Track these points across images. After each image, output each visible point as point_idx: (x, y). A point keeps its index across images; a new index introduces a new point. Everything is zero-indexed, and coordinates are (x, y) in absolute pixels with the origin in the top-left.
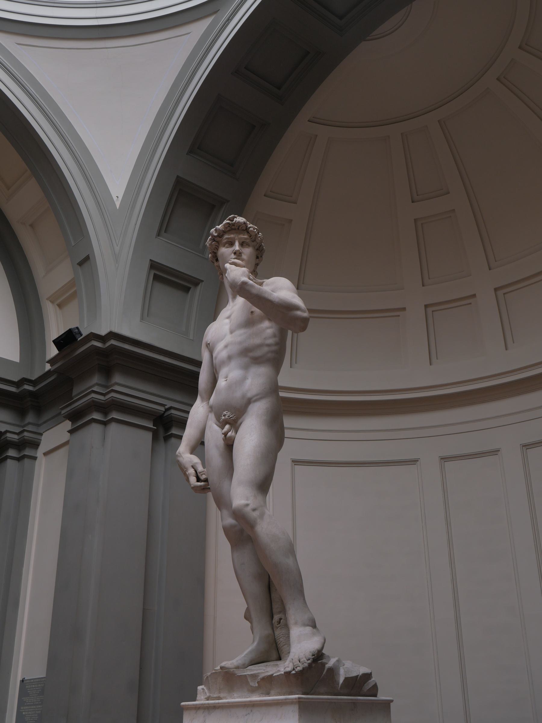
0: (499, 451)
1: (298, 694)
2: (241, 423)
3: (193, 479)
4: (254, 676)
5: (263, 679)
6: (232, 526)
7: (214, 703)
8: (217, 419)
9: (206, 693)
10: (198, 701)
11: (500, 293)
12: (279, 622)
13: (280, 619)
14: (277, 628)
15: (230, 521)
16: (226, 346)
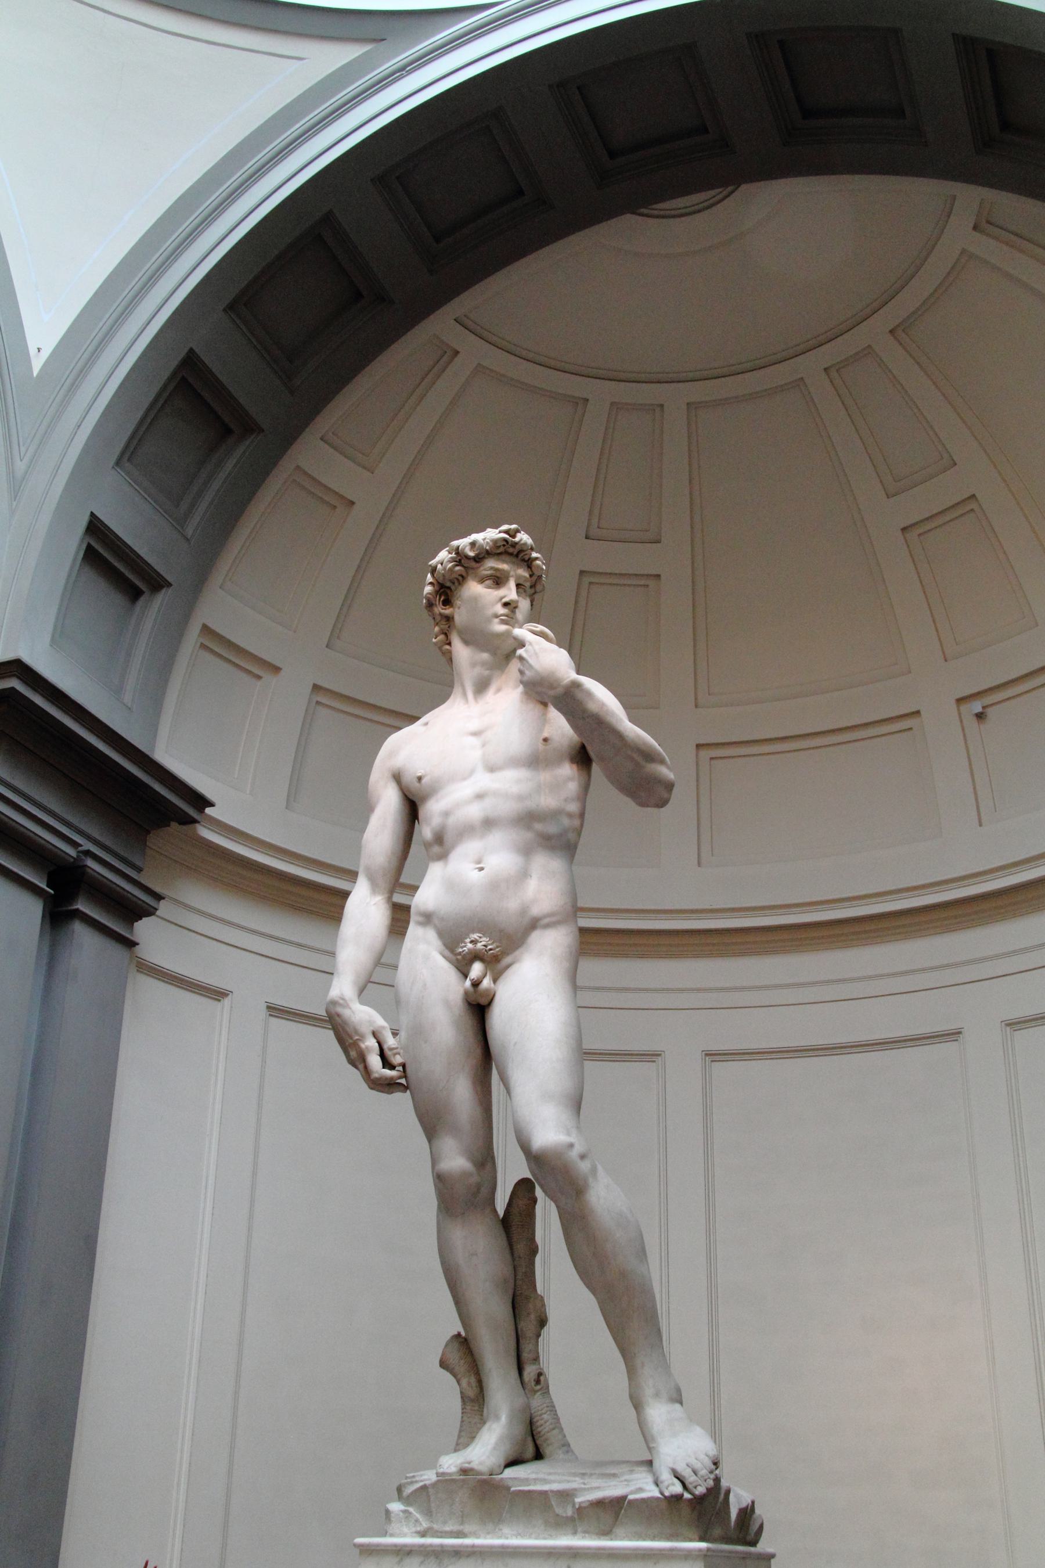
0: (659, 1055)
1: (691, 1540)
2: (508, 966)
3: (374, 1061)
4: (566, 1496)
5: (600, 1503)
6: (465, 1174)
7: (461, 1546)
8: (445, 945)
9: (417, 1521)
10: (392, 1535)
11: (705, 754)
12: (538, 1382)
13: (540, 1374)
14: (536, 1392)
15: (456, 1161)
16: (480, 796)
